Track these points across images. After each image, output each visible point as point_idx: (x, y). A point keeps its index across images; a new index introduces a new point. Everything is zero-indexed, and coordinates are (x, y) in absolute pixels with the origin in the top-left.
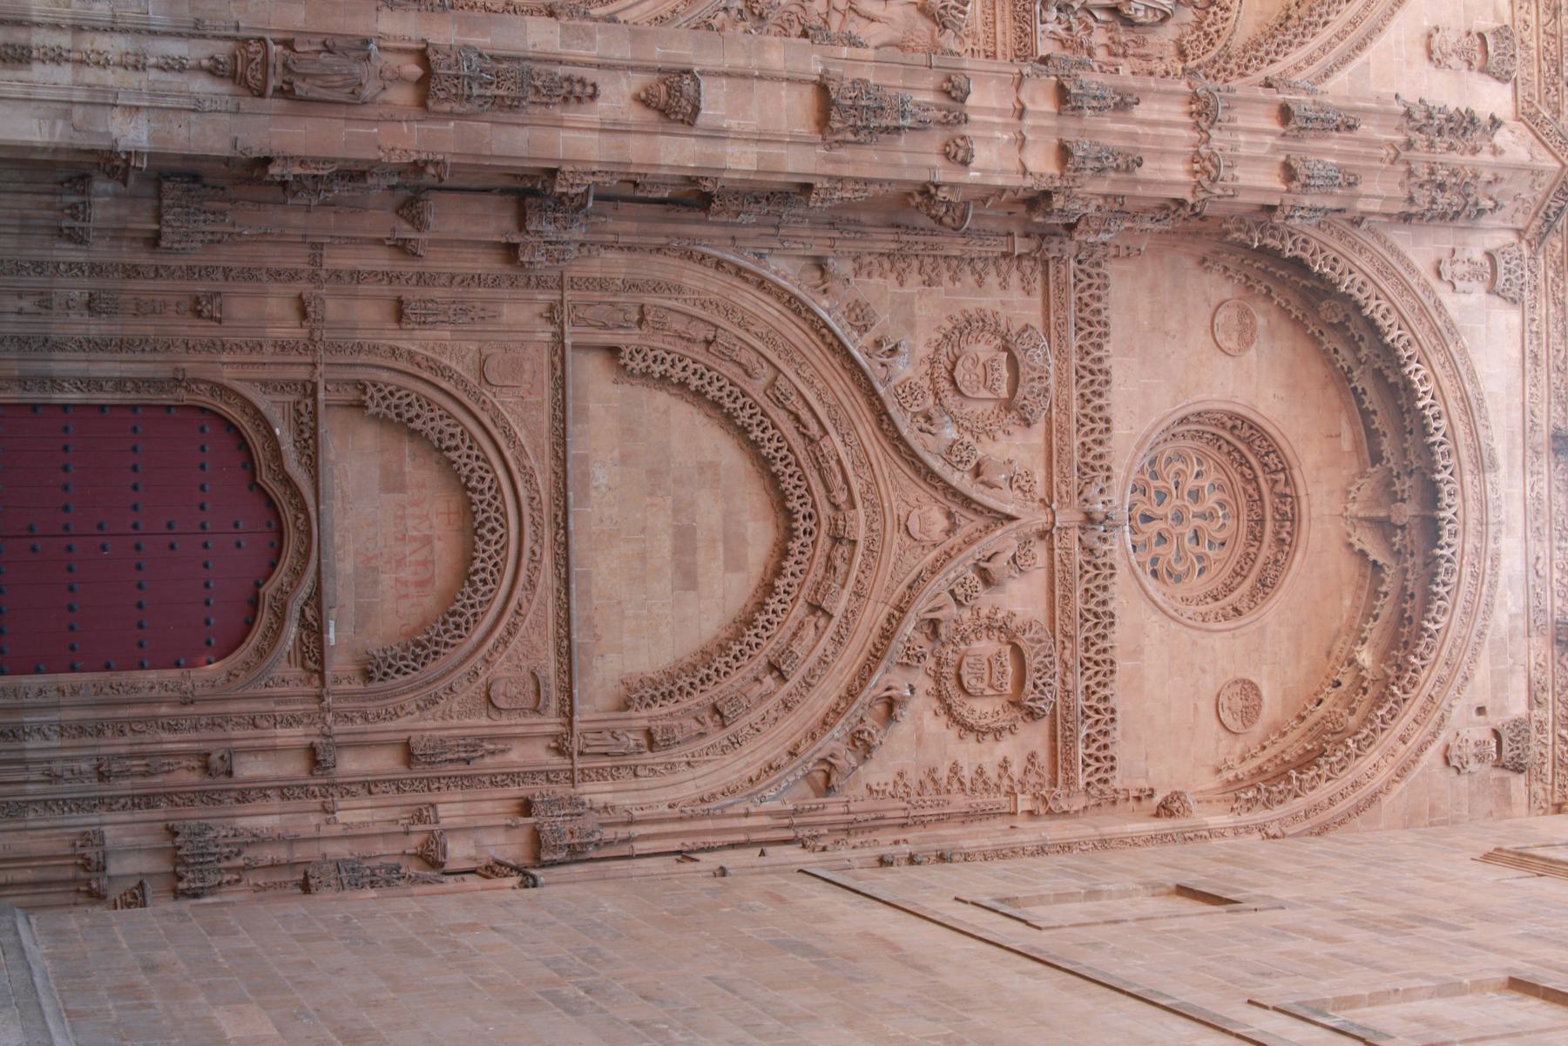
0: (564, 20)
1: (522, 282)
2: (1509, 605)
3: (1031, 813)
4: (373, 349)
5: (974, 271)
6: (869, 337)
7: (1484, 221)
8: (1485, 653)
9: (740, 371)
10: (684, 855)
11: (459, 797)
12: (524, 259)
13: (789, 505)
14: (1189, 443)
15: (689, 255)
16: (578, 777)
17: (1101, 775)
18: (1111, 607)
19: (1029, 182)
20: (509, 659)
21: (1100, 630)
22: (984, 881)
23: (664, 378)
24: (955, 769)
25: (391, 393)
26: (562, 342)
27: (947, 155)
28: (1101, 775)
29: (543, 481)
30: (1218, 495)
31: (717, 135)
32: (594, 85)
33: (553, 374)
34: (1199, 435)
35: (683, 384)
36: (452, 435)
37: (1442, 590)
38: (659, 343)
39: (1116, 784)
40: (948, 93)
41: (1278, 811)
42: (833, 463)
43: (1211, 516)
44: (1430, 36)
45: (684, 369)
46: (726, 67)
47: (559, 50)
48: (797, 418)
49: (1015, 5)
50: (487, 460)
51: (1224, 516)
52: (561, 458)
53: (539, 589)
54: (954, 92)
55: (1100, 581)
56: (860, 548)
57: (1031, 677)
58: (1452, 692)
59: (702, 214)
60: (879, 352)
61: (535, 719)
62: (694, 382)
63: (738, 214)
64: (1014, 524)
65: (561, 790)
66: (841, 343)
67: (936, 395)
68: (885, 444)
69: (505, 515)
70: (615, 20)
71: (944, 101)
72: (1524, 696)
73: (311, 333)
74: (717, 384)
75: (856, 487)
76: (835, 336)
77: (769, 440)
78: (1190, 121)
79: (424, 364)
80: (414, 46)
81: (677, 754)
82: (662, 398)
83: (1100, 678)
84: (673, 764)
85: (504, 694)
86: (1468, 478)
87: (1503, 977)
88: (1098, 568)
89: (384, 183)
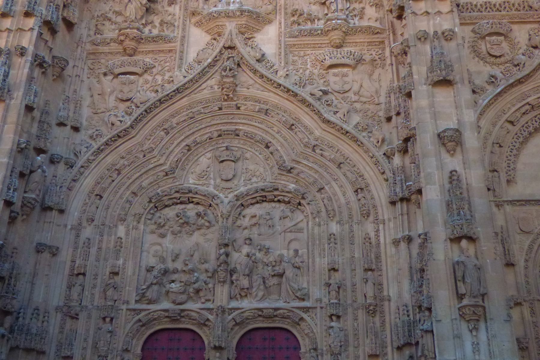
6: (488, 87)
26: (511, 201)
27: (451, 39)
32: (451, 172)
33: (524, 205)
38: (505, 165)
47: (437, 186)
48: (524, 113)
49: (350, 34)
54: (423, 37)
60: (496, 82)
62: (515, 152)
68: (529, 81)
71: (428, 42)
73: (525, 301)
74: (514, 144)
77: (533, 124)
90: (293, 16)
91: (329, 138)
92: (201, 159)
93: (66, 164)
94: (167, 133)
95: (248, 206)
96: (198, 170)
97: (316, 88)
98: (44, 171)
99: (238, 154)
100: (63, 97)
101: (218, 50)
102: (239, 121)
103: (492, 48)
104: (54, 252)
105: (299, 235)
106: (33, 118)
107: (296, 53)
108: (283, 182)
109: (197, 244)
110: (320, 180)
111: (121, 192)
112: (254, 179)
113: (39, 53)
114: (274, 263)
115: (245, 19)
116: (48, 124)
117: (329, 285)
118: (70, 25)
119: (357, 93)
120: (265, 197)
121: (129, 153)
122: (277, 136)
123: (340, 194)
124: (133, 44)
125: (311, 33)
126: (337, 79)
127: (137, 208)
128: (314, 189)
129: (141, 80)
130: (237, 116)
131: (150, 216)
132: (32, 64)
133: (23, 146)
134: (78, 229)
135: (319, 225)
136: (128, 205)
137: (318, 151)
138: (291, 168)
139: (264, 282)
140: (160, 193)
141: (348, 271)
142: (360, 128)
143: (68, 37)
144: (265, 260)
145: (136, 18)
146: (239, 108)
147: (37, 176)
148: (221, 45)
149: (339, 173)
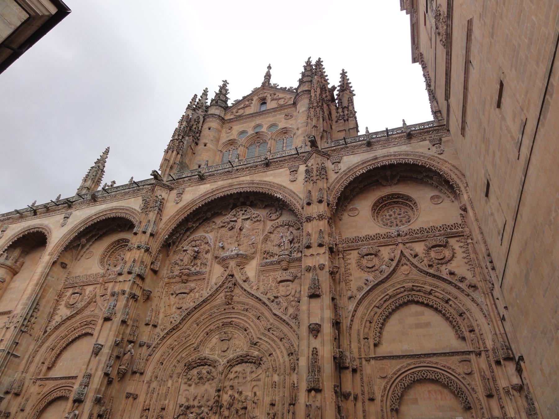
0: (299, 356)
1: (361, 368)
2: (405, 148)
3: (472, 239)
4: (382, 406)
5: (347, 265)
6: (364, 286)
7: (326, 166)
8: (416, 151)
9: (376, 315)
10: (503, 319)
11: (499, 381)
12: (355, 367)
13: (406, 301)
14: (379, 219)
15: (351, 328)
16: (486, 349)
17: (459, 225)
18: (418, 228)
19: (327, 252)
20: (457, 368)
21: (424, 230)
22: (494, 241)
23: (380, 333)
24: (464, 258)
25: (392, 401)
27: (323, 269)
28: (459, 225)
29: (409, 361)
30: (390, 211)
31: (322, 319)
32: (313, 348)
34: (377, 217)
35: (381, 328)
36: (401, 385)
37: (404, 161)
38: (371, 334)
39: (460, 222)
40: (310, 270)
41: (461, 185)
42: (395, 292)
43: (394, 212)
44: (292, 181)
45: (377, 328)
46: (307, 318)
48: (385, 301)
50: (406, 376)
51: (394, 209)
52: (403, 357)
53: (438, 361)
54: (309, 269)
55: (413, 231)
56: (414, 284)
57: (438, 243)
58: (426, 155)
59: (341, 324)
61: (472, 361)
62: (380, 325)
63: (340, 316)
64: (403, 251)
65: (491, 353)
66: (367, 292)
67: (376, 270)
69: (419, 371)
70: (299, 345)
72: (424, 142)
74: (380, 320)
75: (399, 286)
76: (365, 293)
78: (312, 221)
79: (384, 393)
80: (307, 393)
81: (474, 324)
82: (385, 333)
83: (436, 229)
84: (477, 325)
85: (467, 369)
86: (379, 160)
87: (497, 109)
88: (411, 232)
89: (340, 402)
90: (264, 254)
91: (277, 323)
92: (213, 339)
93: (147, 346)
94: (198, 325)
95: (234, 366)
96: (210, 345)
97: (271, 295)
98: (131, 353)
99: (230, 336)
100: (150, 309)
101: (225, 277)
102: (233, 316)
103: (367, 263)
104: (135, 397)
105: (258, 383)
106: (128, 325)
107: (265, 275)
108: (252, 351)
109: (206, 390)
110: (270, 348)
111: (172, 360)
112: (238, 350)
113: (132, 292)
114: (244, 401)
115: (239, 259)
116: (136, 326)
117: (268, 414)
118: (155, 272)
119: (294, 296)
120: (242, 360)
121: (179, 337)
122: (251, 323)
123: (280, 357)
124: (184, 277)
125: (272, 263)
126: (284, 288)
127: (179, 370)
128: (267, 355)
129: (189, 296)
130: (232, 314)
131: (185, 374)
132: (128, 298)
133: (118, 342)
134: (149, 382)
135: (268, 377)
136: (174, 368)
137: (271, 331)
138: (256, 343)
139: (237, 412)
140: (191, 361)
141: (280, 405)
142: (292, 317)
143: (155, 277)
144: (239, 399)
145: (188, 263)
146: (234, 309)
147: (126, 357)
148: (227, 274)
149: (280, 343)
